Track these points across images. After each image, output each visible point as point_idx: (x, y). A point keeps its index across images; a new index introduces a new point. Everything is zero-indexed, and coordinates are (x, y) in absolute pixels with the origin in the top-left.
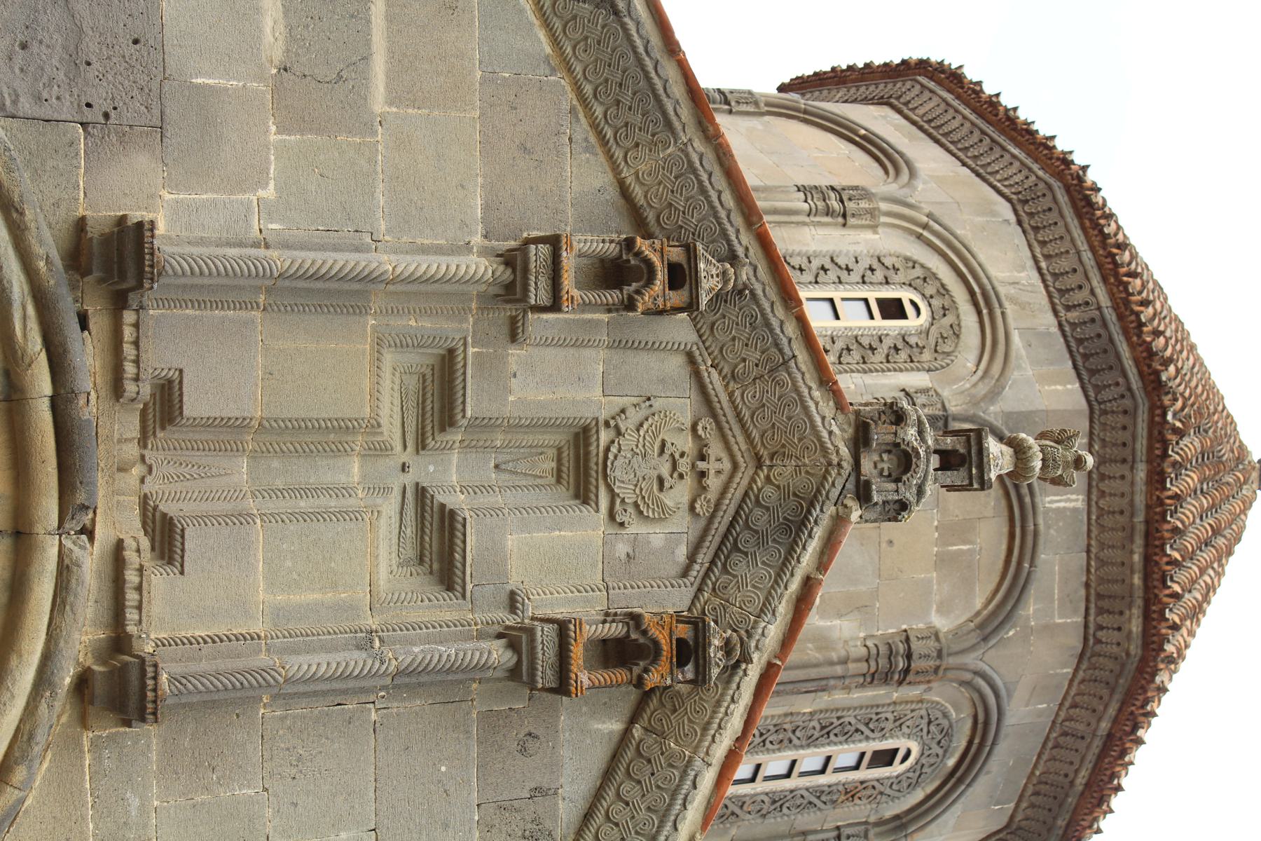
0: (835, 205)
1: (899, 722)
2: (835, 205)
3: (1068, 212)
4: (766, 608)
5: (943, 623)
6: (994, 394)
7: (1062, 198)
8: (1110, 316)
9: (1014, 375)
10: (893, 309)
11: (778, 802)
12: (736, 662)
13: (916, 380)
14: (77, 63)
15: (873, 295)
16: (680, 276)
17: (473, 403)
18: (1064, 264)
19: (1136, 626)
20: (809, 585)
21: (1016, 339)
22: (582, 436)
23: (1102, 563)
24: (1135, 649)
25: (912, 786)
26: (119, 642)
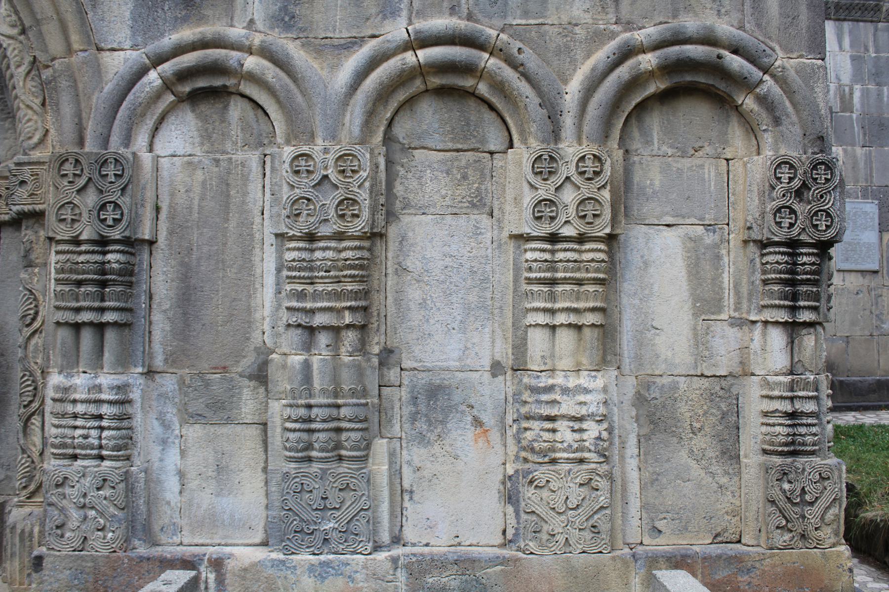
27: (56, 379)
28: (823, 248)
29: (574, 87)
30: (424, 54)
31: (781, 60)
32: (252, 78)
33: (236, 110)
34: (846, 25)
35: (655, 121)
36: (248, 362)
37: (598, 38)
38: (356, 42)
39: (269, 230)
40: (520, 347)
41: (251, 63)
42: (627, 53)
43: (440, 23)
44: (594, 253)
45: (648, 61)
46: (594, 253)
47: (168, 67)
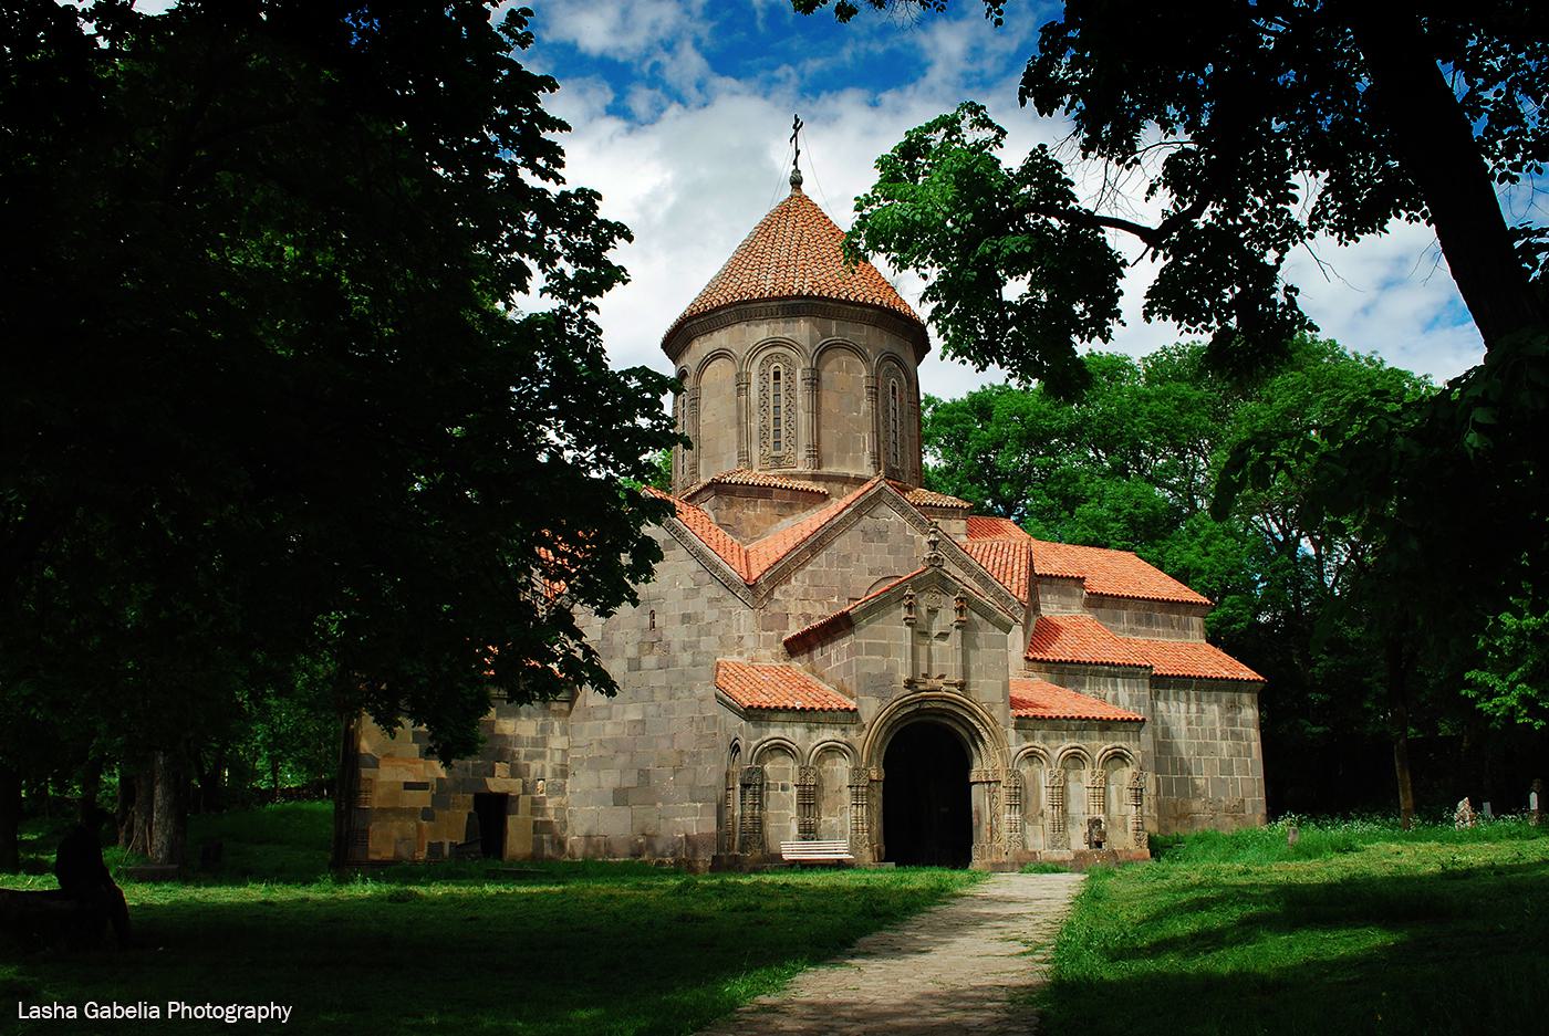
0: (744, 386)
1: (887, 387)
2: (744, 386)
3: (748, 306)
4: (955, 584)
5: (864, 373)
6: (805, 351)
7: (742, 307)
8: (782, 303)
9: (798, 340)
10: (777, 375)
11: (902, 423)
12: (963, 592)
13: (799, 372)
14: (884, 685)
15: (772, 382)
16: (911, 597)
17: (926, 630)
18: (764, 312)
19: (870, 311)
20: (953, 577)
21: (787, 335)
22: (928, 611)
23: (852, 317)
24: (877, 312)
25: (901, 379)
26: (955, 685)
27: (1007, 815)
28: (1141, 790)
29: (1097, 757)
30: (1071, 751)
31: (1133, 752)
32: (1041, 755)
33: (1035, 759)
34: (1126, 680)
35: (1110, 764)
36: (1040, 812)
37: (1101, 747)
38: (1058, 747)
39: (1044, 785)
40: (1089, 809)
41: (1041, 751)
42: (1106, 750)
43: (1074, 744)
44: (1101, 790)
45: (1110, 752)
46: (1101, 790)
47: (1025, 751)
